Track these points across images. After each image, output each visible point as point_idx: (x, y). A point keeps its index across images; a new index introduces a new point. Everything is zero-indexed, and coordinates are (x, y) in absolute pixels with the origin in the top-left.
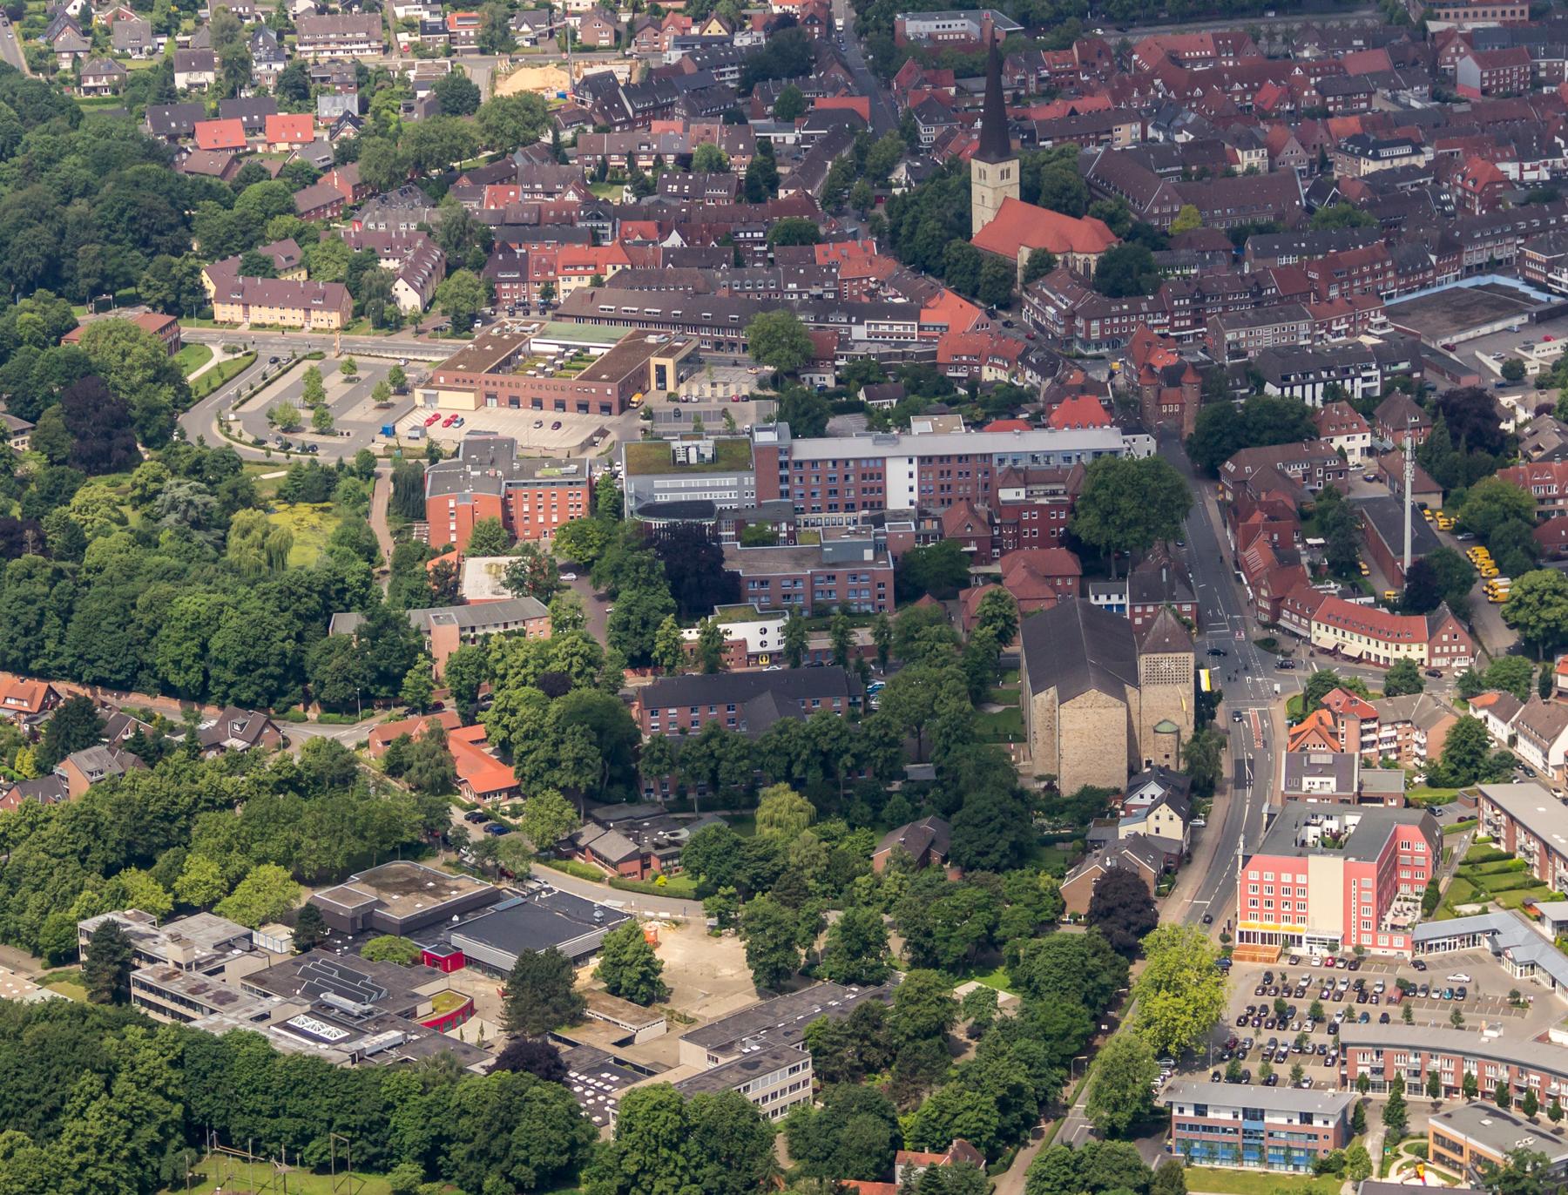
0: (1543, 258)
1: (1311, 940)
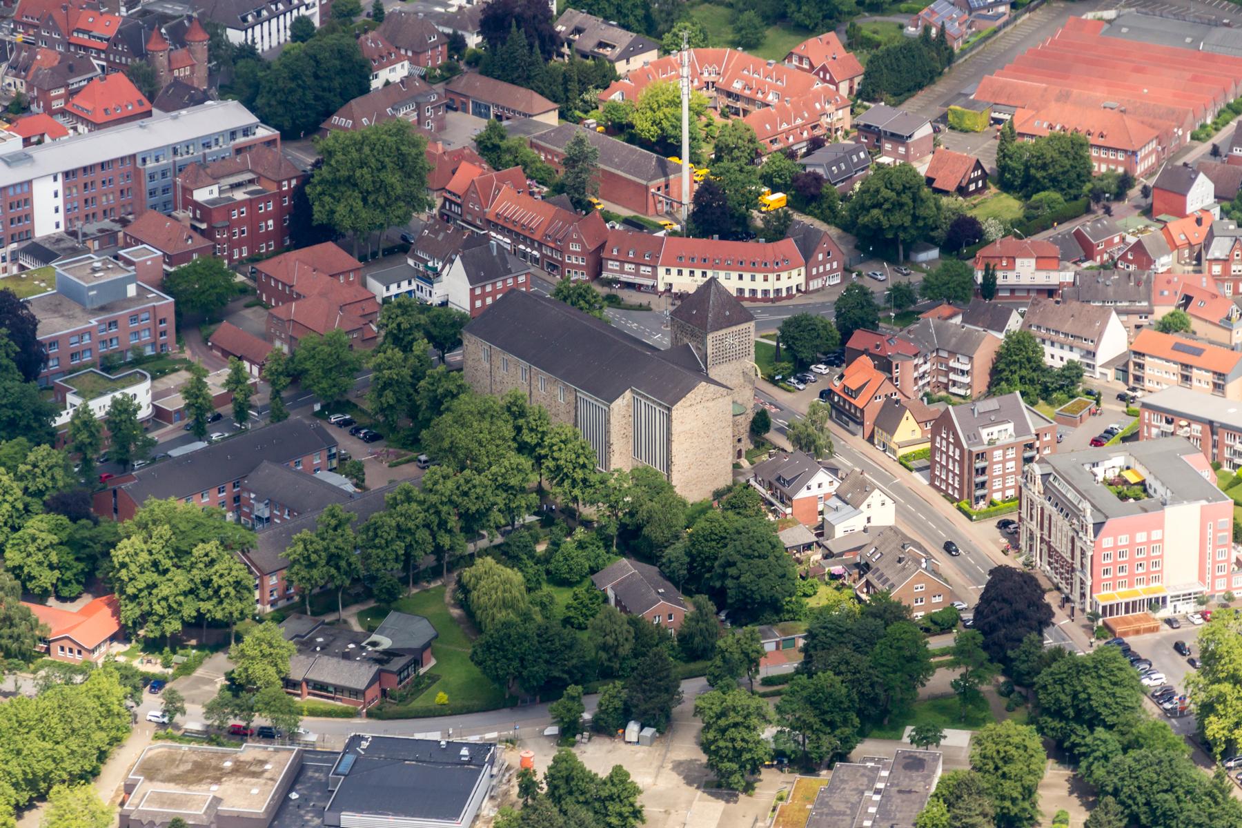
1: (1176, 598)
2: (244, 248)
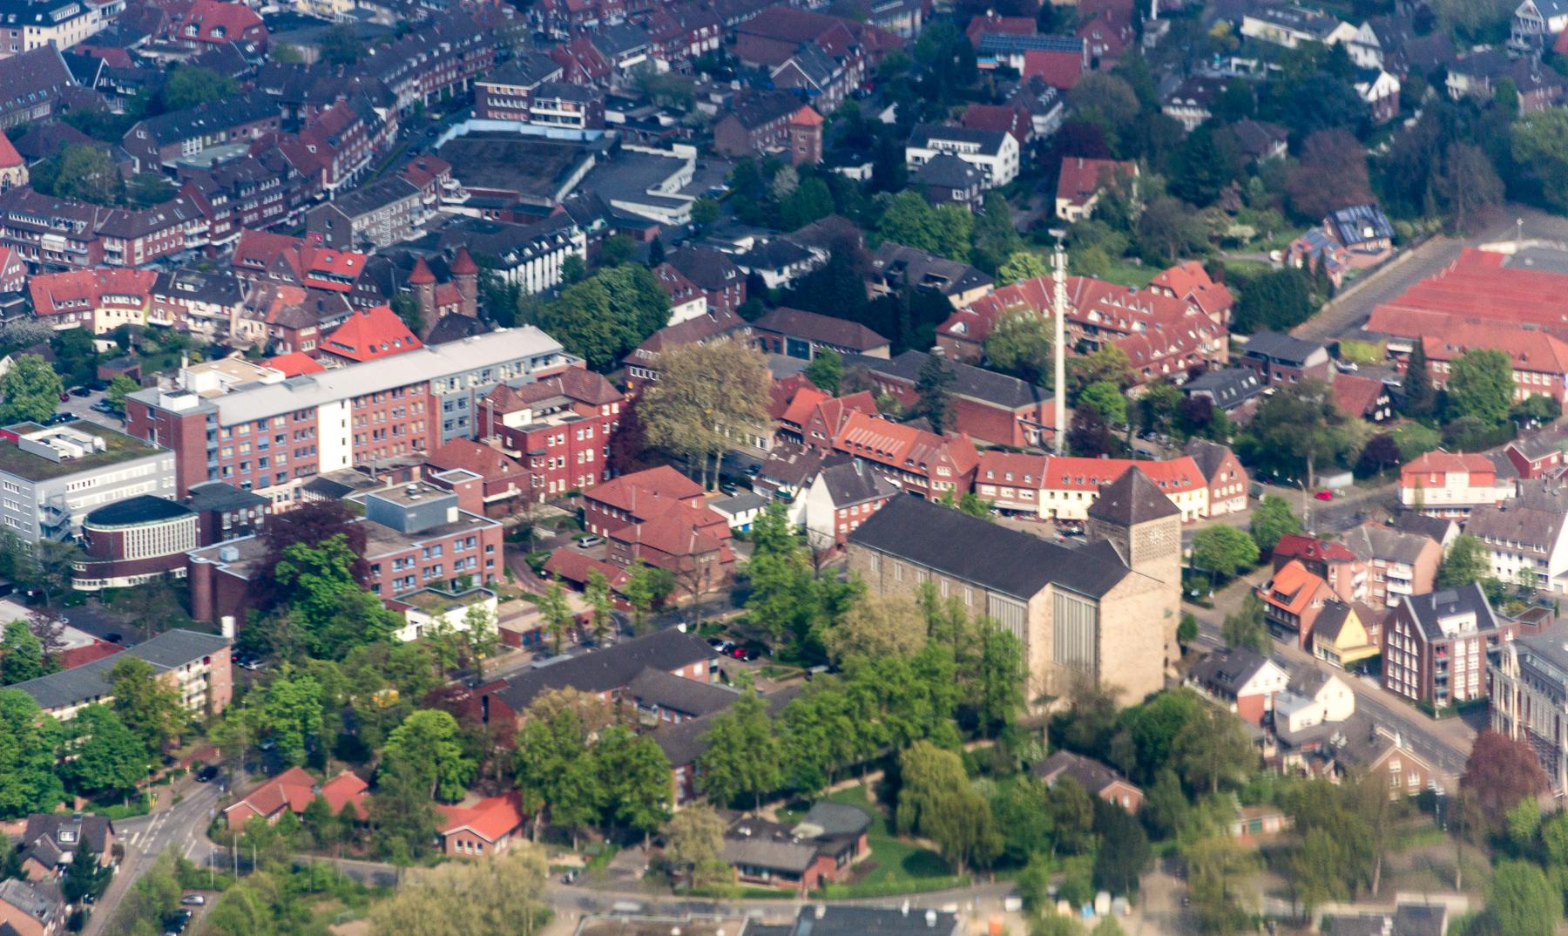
0: (522, 90)
2: (562, 482)
